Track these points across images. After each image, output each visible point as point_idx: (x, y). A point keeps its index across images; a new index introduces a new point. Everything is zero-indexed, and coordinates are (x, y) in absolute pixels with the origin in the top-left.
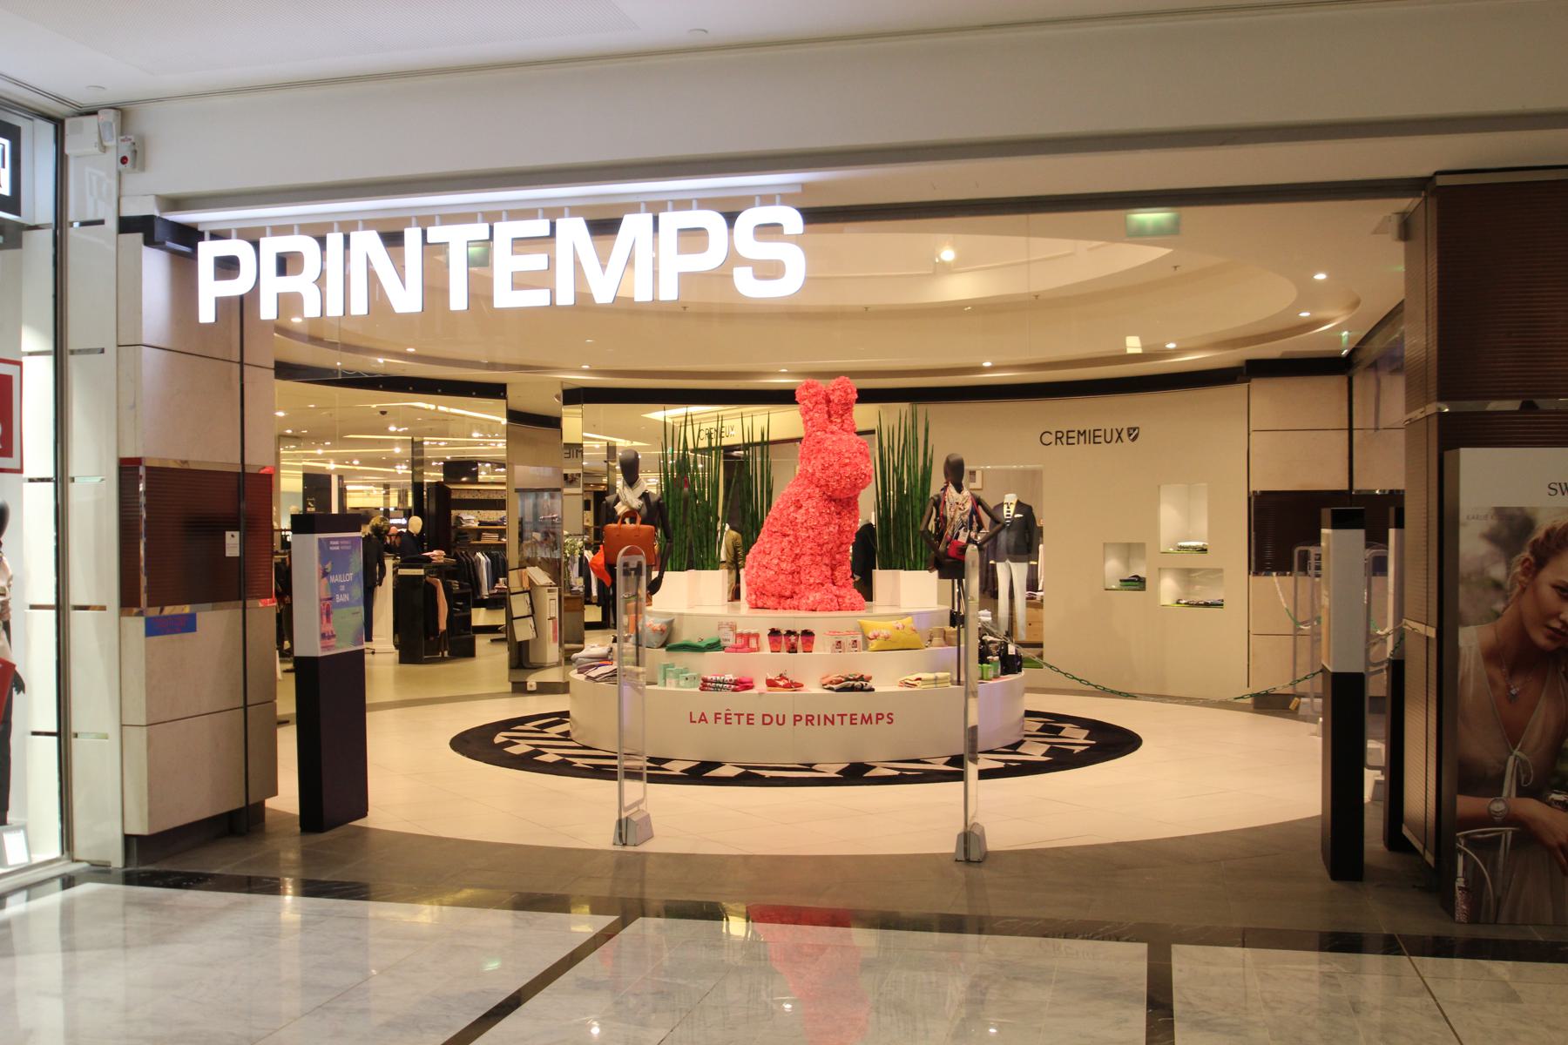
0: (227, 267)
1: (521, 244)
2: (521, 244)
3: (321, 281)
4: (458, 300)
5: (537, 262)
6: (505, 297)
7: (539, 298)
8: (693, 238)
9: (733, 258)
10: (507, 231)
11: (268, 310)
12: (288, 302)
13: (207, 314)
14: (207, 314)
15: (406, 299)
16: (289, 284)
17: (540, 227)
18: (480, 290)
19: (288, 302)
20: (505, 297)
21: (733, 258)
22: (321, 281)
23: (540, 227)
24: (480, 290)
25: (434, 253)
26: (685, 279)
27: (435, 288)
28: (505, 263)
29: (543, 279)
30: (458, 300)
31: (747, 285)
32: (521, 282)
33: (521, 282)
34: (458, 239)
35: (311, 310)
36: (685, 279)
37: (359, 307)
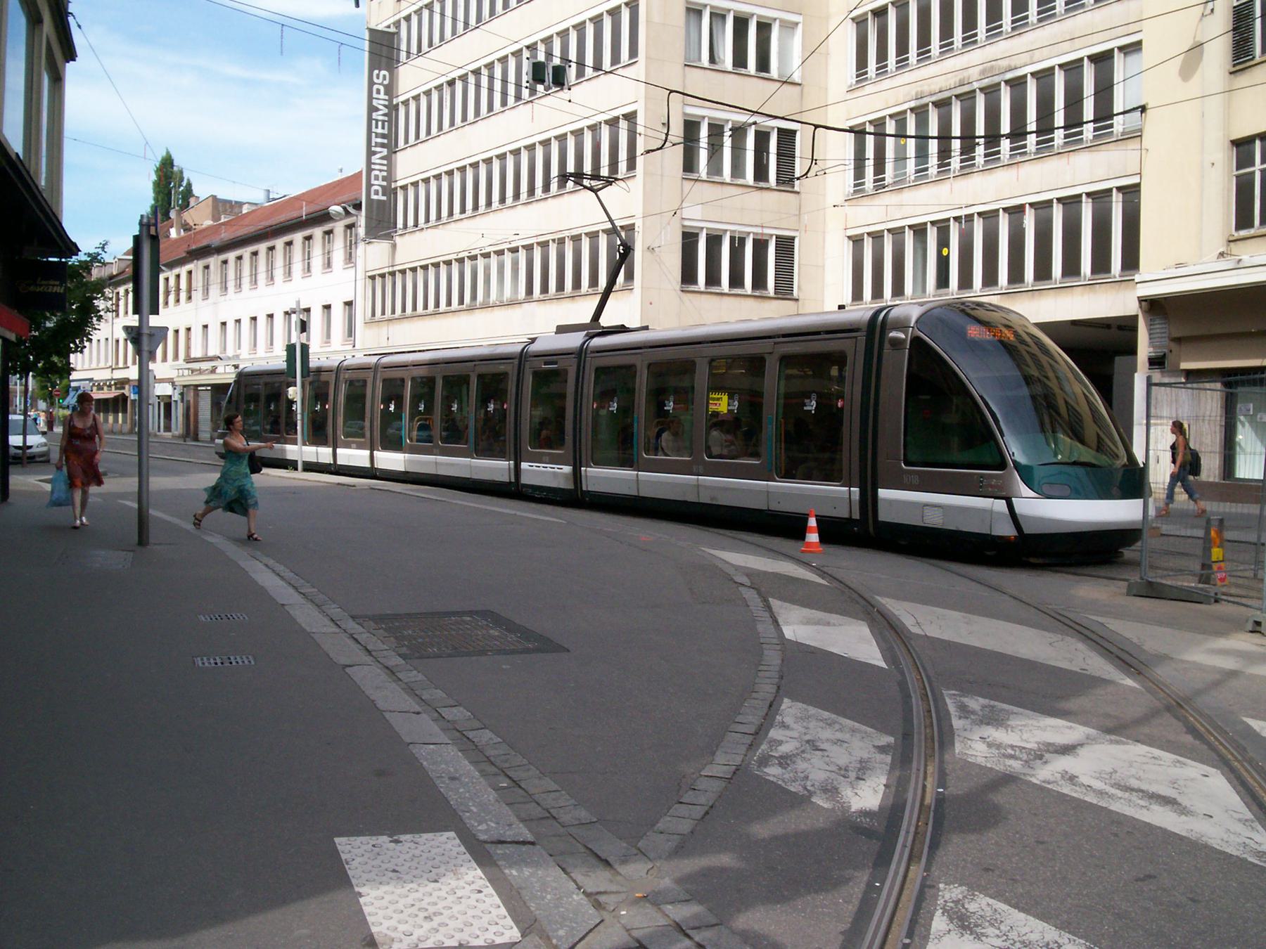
0: (377, 193)
1: (377, 127)
3: (381, 171)
5: (380, 123)
6: (386, 131)
7: (386, 123)
11: (385, 183)
13: (384, 198)
14: (384, 198)
17: (374, 122)
18: (383, 136)
22: (381, 171)
23: (374, 122)
24: (383, 136)
25: (377, 145)
26: (385, 94)
27: (383, 145)
28: (380, 130)
31: (386, 82)
32: (383, 128)
34: (375, 140)
35: (385, 174)
37: (385, 162)
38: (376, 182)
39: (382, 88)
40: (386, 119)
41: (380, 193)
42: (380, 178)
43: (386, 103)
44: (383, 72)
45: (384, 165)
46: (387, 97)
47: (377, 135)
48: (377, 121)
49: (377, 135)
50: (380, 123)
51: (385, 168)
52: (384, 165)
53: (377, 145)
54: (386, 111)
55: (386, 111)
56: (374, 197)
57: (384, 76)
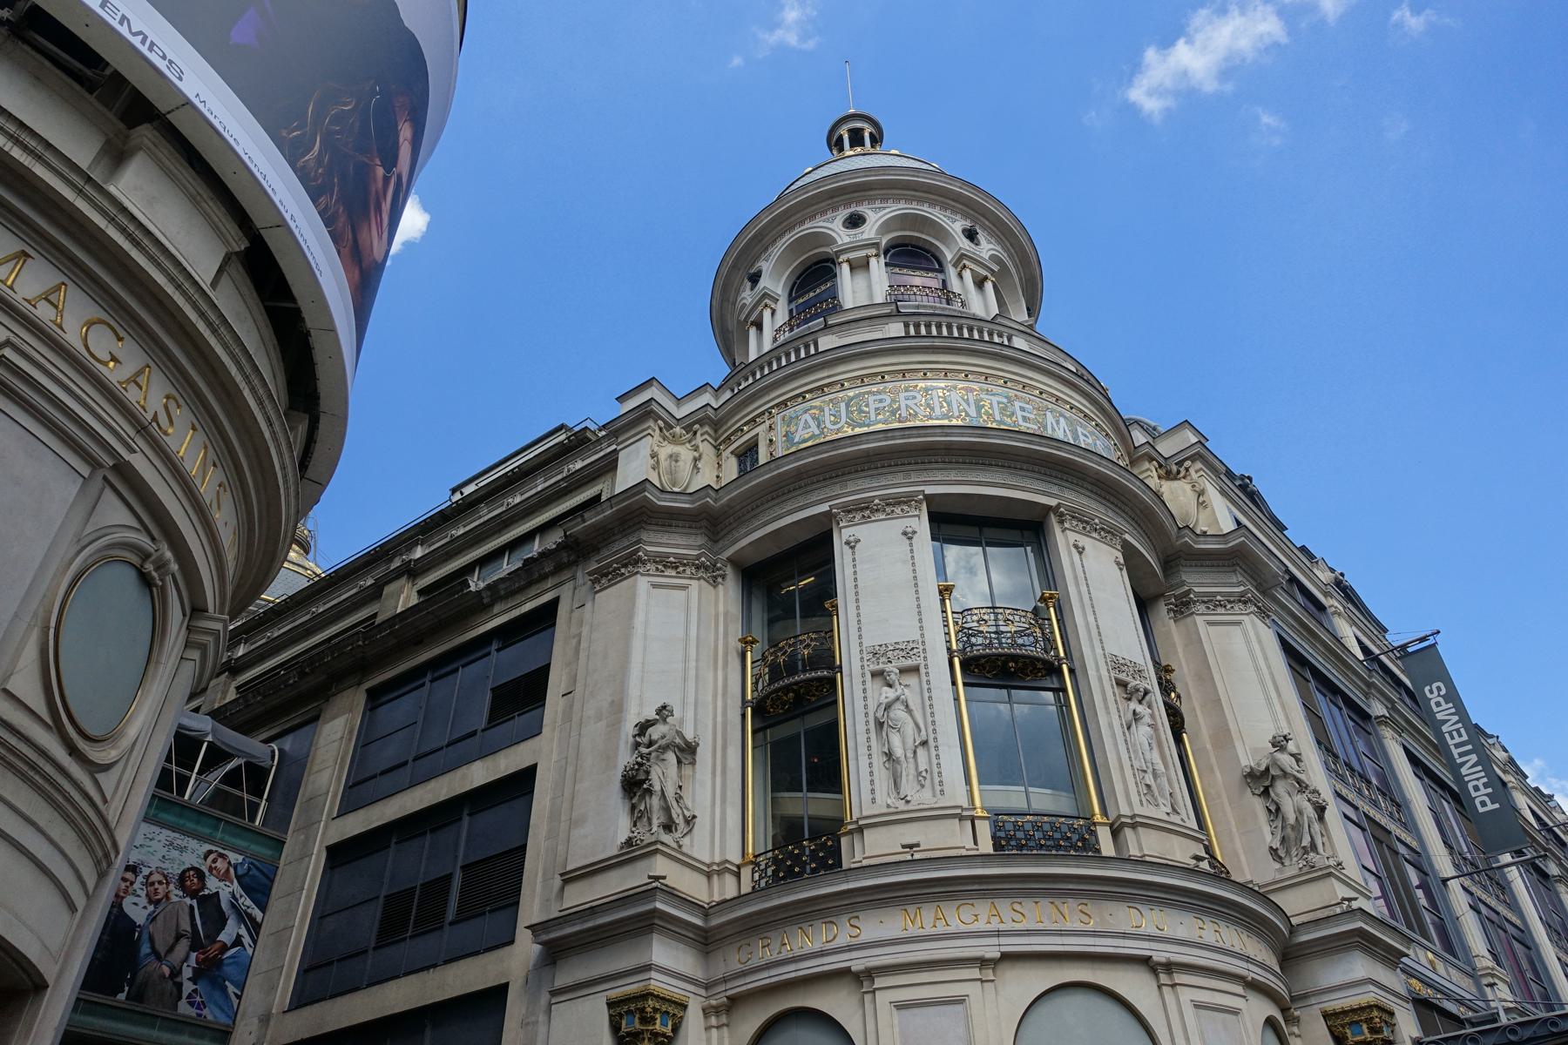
0: (1483, 804)
1: (1453, 738)
2: (1453, 738)
3: (1477, 779)
4: (1470, 747)
5: (1455, 733)
6: (1465, 738)
7: (1462, 730)
8: (1438, 704)
9: (1439, 695)
10: (1450, 742)
11: (1490, 790)
12: (1486, 785)
13: (1497, 806)
14: (1497, 806)
15: (1474, 758)
16: (1481, 787)
17: (1447, 735)
19: (1486, 785)
20: (1465, 738)
21: (1439, 695)
22: (1477, 779)
25: (1461, 755)
26: (1447, 703)
28: (1457, 740)
29: (1458, 731)
30: (1470, 747)
31: (1443, 692)
32: (1460, 735)
33: (1460, 735)
34: (1455, 752)
35: (1485, 780)
36: (1447, 703)
37: (1480, 768)
38: (1478, 793)
39: (1441, 699)
40: (1460, 725)
41: (1488, 802)
42: (1481, 787)
43: (1453, 710)
44: (1434, 686)
45: (1480, 771)
46: (1451, 705)
47: (1457, 746)
48: (1450, 733)
49: (1457, 746)
50: (1455, 733)
51: (1483, 774)
52: (1480, 771)
53: (1461, 755)
54: (1456, 718)
55: (1456, 718)
56: (1481, 810)
57: (1439, 689)
